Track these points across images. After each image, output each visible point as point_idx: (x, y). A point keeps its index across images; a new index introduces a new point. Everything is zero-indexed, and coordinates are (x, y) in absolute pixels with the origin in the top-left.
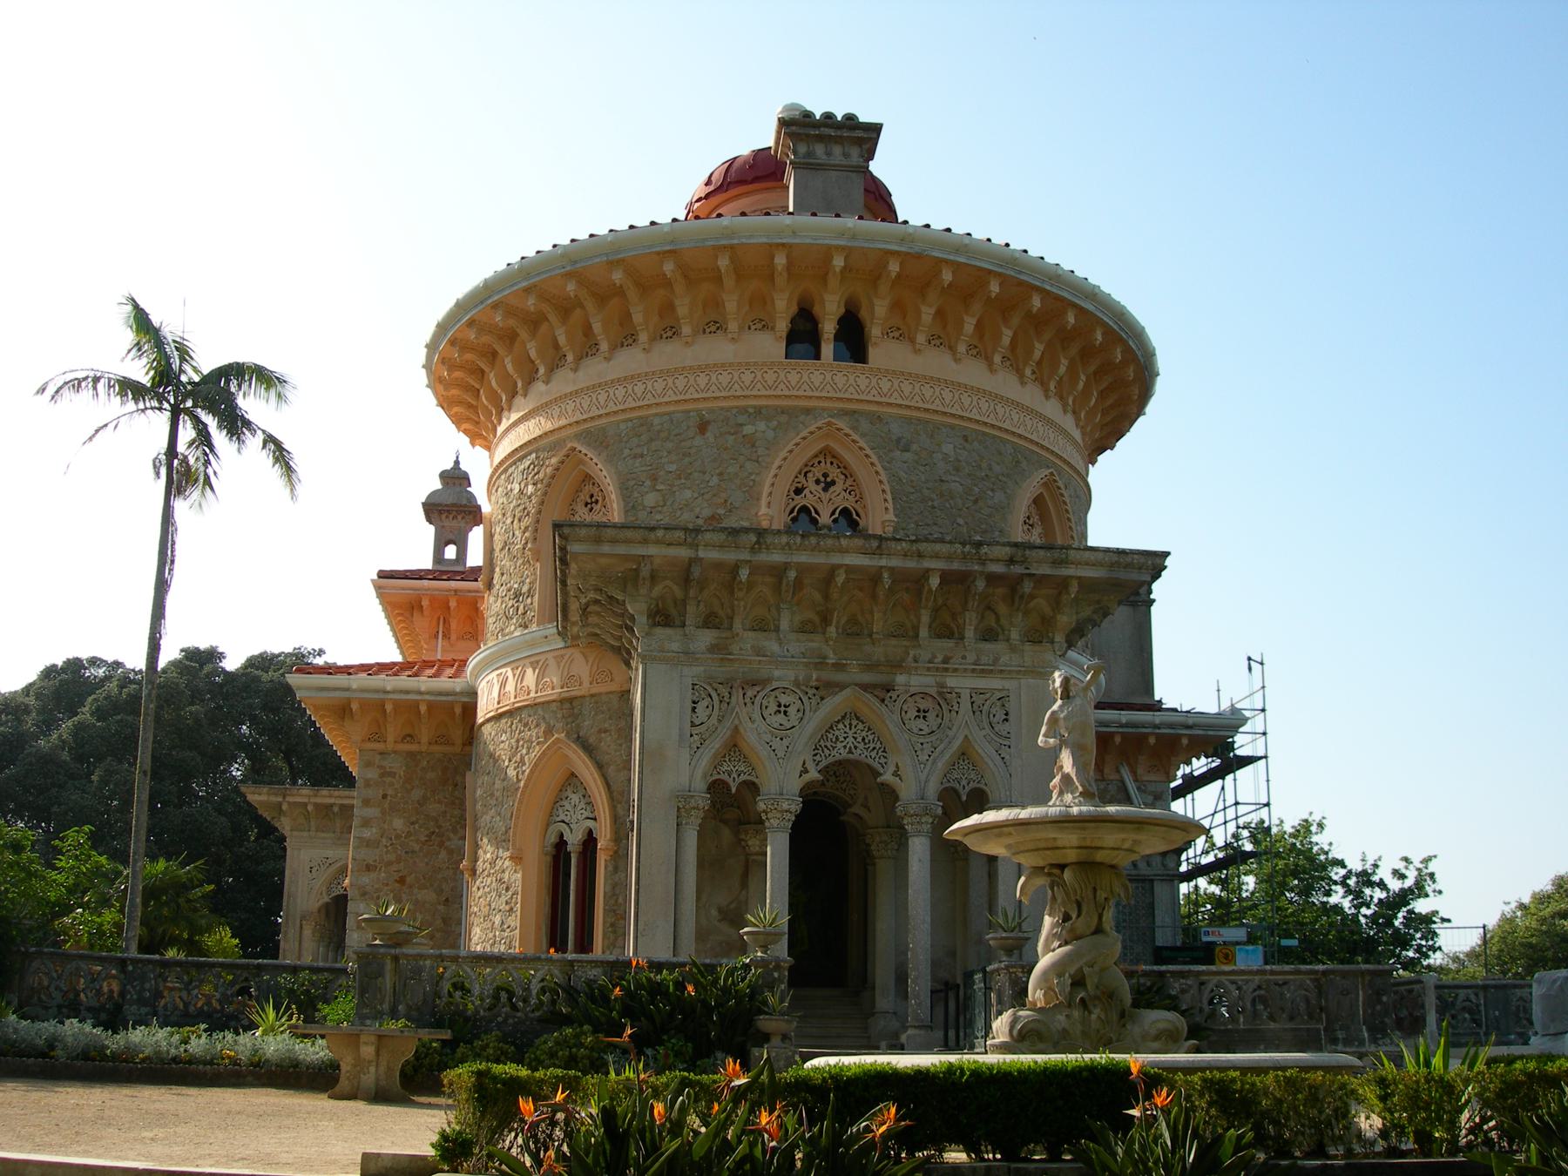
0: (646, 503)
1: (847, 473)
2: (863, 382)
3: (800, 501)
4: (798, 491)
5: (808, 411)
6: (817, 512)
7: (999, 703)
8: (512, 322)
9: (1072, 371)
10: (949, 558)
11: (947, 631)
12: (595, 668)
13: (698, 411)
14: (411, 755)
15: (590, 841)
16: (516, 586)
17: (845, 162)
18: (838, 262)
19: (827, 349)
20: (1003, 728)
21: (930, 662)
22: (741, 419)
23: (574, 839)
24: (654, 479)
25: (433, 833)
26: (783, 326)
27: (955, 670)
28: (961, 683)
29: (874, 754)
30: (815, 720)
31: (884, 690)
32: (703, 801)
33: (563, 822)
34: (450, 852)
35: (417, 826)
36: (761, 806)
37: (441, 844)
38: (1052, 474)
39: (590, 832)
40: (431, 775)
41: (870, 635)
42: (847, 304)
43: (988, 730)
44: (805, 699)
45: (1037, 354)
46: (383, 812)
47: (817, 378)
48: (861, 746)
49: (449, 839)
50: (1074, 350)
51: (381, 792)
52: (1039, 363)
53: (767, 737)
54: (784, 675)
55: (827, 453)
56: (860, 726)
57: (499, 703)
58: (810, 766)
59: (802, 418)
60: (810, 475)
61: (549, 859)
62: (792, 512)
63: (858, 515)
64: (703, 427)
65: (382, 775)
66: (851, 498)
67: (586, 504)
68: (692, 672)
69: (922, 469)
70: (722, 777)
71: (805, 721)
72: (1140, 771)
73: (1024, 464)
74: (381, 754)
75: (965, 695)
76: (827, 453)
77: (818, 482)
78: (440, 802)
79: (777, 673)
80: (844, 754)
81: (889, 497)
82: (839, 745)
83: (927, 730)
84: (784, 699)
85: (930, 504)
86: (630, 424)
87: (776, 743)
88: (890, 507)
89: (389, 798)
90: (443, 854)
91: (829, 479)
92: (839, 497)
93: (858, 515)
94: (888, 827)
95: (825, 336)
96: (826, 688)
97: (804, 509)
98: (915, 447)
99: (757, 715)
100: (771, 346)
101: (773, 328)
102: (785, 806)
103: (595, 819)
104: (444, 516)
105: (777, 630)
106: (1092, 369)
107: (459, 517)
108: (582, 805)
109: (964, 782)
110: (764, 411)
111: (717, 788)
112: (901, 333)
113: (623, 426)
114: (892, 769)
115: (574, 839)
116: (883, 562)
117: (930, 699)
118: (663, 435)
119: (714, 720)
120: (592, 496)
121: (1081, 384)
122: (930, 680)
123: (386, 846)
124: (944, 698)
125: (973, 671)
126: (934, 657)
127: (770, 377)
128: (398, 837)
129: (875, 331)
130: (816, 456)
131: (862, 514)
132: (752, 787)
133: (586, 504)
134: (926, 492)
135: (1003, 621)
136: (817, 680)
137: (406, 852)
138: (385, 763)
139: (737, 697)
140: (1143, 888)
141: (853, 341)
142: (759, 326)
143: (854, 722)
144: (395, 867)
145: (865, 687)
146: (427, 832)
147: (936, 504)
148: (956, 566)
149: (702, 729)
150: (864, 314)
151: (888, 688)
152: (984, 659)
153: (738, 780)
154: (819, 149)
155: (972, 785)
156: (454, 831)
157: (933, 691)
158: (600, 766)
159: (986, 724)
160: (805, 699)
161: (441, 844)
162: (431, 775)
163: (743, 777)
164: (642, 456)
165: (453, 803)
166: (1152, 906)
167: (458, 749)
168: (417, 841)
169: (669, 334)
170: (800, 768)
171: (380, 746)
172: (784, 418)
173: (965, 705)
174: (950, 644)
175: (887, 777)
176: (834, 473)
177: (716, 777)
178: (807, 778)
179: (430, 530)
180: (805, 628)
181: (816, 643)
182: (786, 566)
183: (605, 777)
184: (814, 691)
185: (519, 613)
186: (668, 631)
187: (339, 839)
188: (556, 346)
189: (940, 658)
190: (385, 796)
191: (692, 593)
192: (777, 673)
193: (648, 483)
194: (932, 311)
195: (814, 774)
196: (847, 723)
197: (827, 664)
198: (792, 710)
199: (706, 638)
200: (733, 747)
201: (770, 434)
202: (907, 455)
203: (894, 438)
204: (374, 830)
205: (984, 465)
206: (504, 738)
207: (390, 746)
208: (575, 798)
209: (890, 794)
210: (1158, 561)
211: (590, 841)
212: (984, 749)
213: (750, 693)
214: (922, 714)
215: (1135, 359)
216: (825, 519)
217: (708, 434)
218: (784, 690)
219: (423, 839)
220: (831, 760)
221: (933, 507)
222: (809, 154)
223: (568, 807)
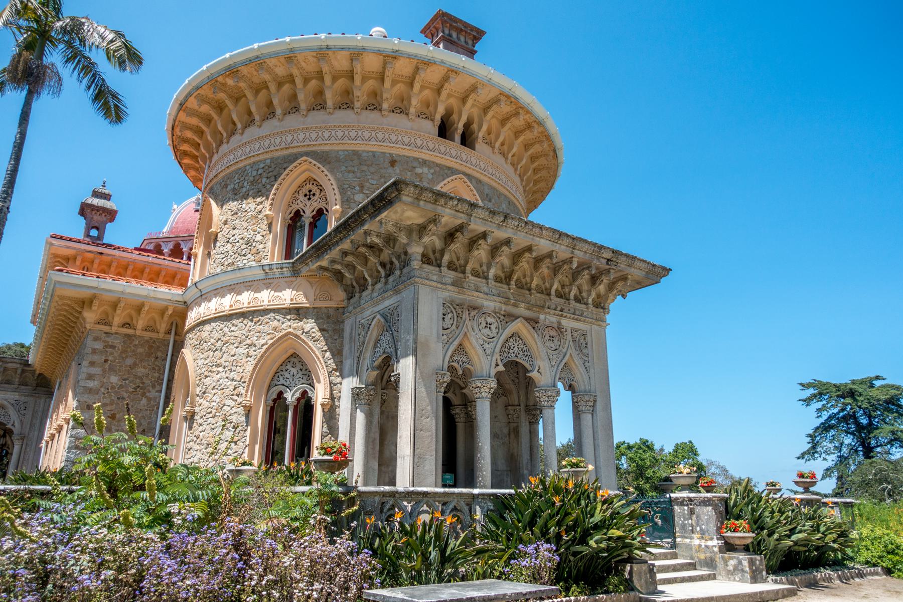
0: (355, 199)
5: (449, 168)
8: (267, 77)
12: (318, 292)
13: (391, 155)
14: (128, 336)
20: (585, 351)
22: (416, 164)
23: (291, 397)
24: (362, 187)
25: (139, 387)
26: (438, 118)
27: (565, 317)
29: (527, 358)
31: (533, 322)
33: (283, 385)
34: (149, 399)
35: (127, 382)
37: (143, 395)
40: (140, 350)
41: (530, 290)
46: (104, 371)
48: (521, 353)
49: (150, 392)
51: (104, 358)
56: (520, 341)
57: (231, 306)
59: (446, 171)
61: (269, 408)
64: (393, 163)
65: (106, 346)
67: (306, 195)
71: (499, 335)
74: (105, 333)
78: (145, 368)
79: (486, 303)
82: (511, 351)
83: (554, 348)
84: (489, 320)
87: (486, 345)
89: (109, 362)
90: (144, 401)
95: (459, 131)
96: (510, 317)
98: (493, 201)
100: (431, 128)
104: (94, 212)
105: (486, 278)
107: (103, 215)
108: (300, 375)
110: (427, 163)
111: (451, 369)
114: (537, 368)
115: (291, 397)
119: (454, 327)
120: (310, 191)
123: (104, 394)
124: (560, 329)
125: (573, 319)
126: (557, 307)
128: (113, 388)
129: (481, 135)
133: (306, 195)
135: (584, 294)
136: (505, 311)
137: (118, 398)
138: (107, 339)
139: (465, 315)
143: (518, 339)
144: (108, 408)
145: (527, 319)
146: (134, 386)
149: (448, 331)
152: (577, 313)
156: (154, 386)
157: (555, 326)
161: (143, 395)
162: (140, 350)
165: (154, 369)
167: (161, 336)
168: (127, 392)
169: (372, 108)
170: (494, 363)
171: (106, 328)
172: (438, 169)
173: (569, 337)
174: (563, 301)
179: (82, 222)
180: (497, 279)
184: (502, 317)
185: (252, 252)
186: (431, 268)
187: (35, 390)
188: (250, 113)
189: (559, 308)
190: (106, 361)
193: (357, 188)
195: (501, 368)
198: (493, 327)
199: (450, 275)
201: (430, 176)
204: (96, 382)
207: (114, 329)
208: (294, 371)
213: (473, 313)
218: (489, 315)
219: (131, 390)
220: (508, 359)
222: (450, 35)
223: (287, 375)
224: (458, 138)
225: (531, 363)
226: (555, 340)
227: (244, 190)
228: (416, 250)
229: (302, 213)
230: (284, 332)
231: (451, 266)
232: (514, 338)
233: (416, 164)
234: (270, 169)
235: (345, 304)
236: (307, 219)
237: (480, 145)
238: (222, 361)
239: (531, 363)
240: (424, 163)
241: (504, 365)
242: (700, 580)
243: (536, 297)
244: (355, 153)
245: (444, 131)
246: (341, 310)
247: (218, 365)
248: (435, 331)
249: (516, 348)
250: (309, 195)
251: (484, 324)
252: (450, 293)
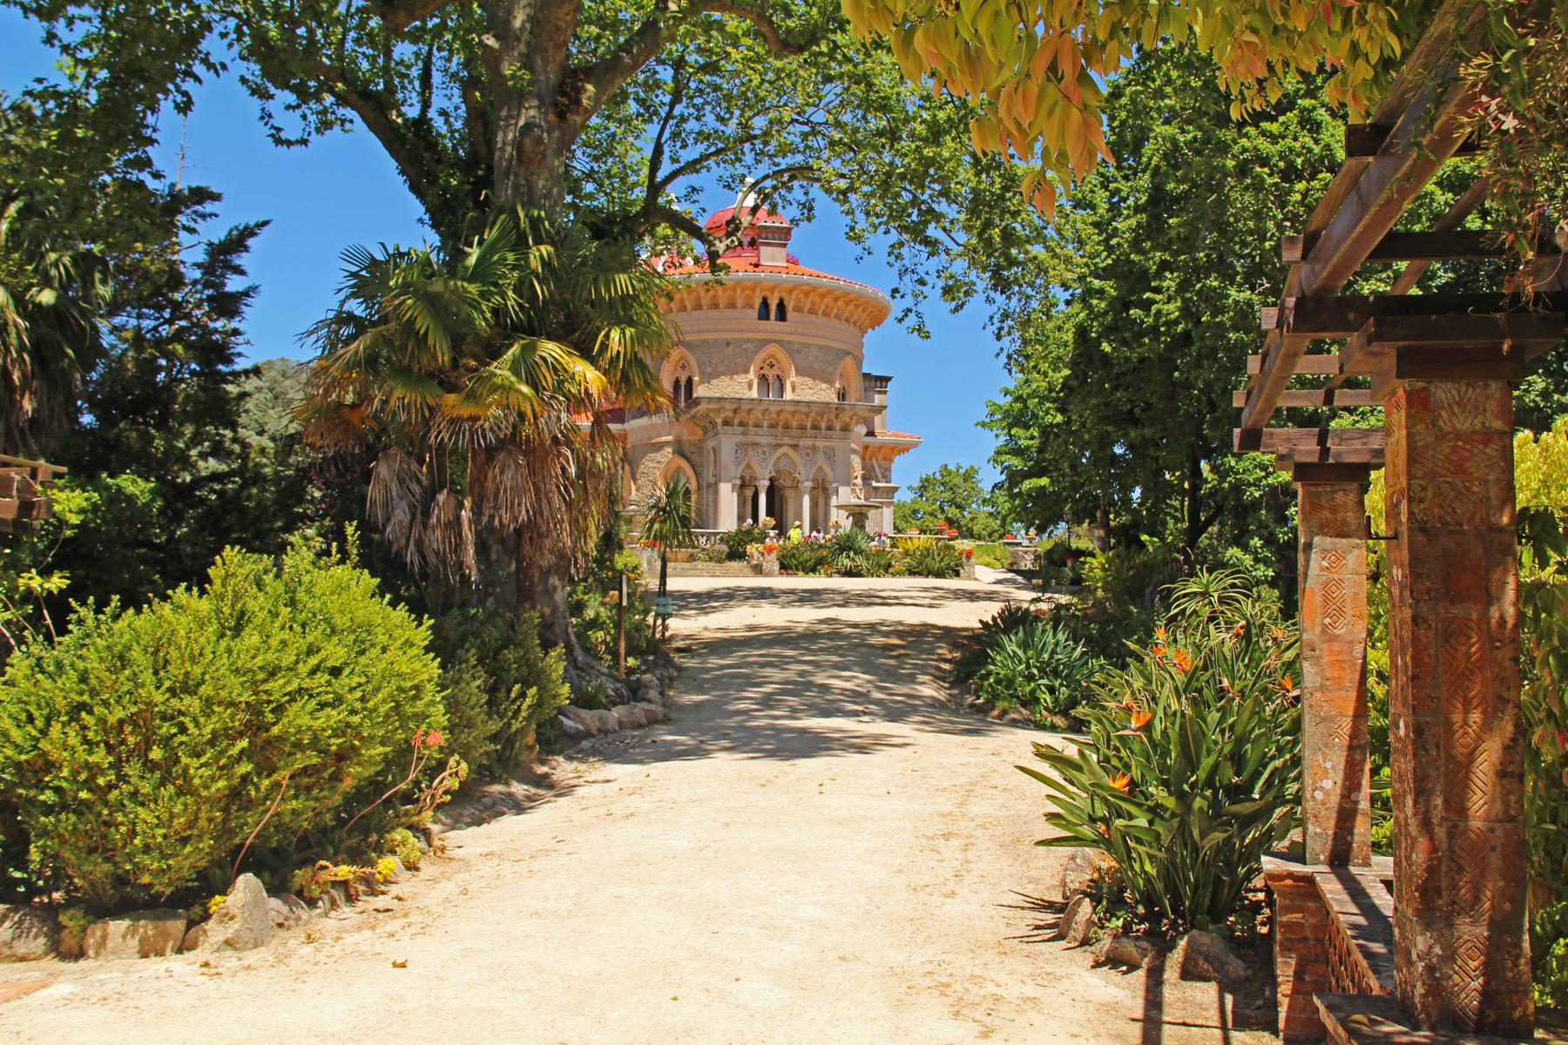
11: (815, 427)
28: (820, 444)
31: (795, 447)
32: (738, 482)
54: (765, 441)
92: (776, 371)
96: (780, 446)
111: (742, 478)
112: (798, 309)
124: (814, 448)
141: (782, 315)
158: (693, 466)
181: (774, 431)
200: (748, 466)
216: (771, 380)
224: (773, 316)
228: (719, 421)
231: (741, 424)
236: (683, 383)
237: (790, 315)
240: (748, 340)
242: (983, 599)
243: (794, 432)
244: (706, 341)
245: (764, 313)
250: (683, 367)
252: (740, 439)
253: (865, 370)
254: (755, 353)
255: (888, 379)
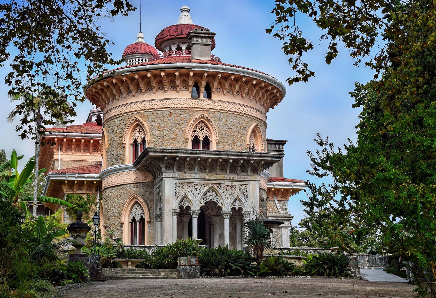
1: (207, 126)
2: (211, 103)
3: (195, 134)
4: (194, 131)
6: (199, 137)
7: (245, 188)
9: (263, 95)
10: (235, 155)
12: (143, 176)
15: (142, 219)
16: (118, 152)
17: (206, 43)
18: (206, 74)
19: (202, 96)
21: (229, 178)
22: (180, 113)
23: (138, 219)
29: (216, 199)
30: (203, 192)
36: (191, 212)
38: (257, 124)
39: (142, 217)
42: (207, 83)
43: (242, 194)
44: (201, 187)
45: (254, 93)
47: (199, 102)
48: (214, 198)
50: (264, 91)
52: (255, 95)
53: (193, 195)
55: (202, 121)
56: (213, 193)
58: (202, 202)
60: (198, 127)
61: (130, 224)
62: (193, 136)
63: (209, 137)
66: (207, 133)
68: (175, 181)
69: (225, 126)
70: (182, 205)
72: (279, 198)
73: (250, 122)
75: (237, 186)
76: (202, 121)
77: (199, 129)
80: (210, 200)
81: (217, 134)
82: (208, 197)
84: (196, 187)
85: (227, 134)
86: (151, 112)
88: (218, 136)
91: (202, 128)
93: (209, 137)
94: (217, 215)
96: (205, 185)
97: (196, 136)
99: (190, 191)
101: (188, 89)
102: (197, 212)
103: (144, 213)
106: (268, 94)
109: (237, 206)
111: (181, 208)
113: (149, 113)
115: (138, 219)
116: (220, 157)
117: (229, 187)
118: (160, 116)
121: (265, 98)
122: (230, 183)
126: (230, 177)
127: (188, 102)
129: (214, 90)
130: (199, 122)
131: (210, 137)
132: (188, 208)
134: (226, 131)
139: (185, 187)
140: (280, 230)
142: (185, 88)
143: (212, 192)
147: (229, 134)
148: (236, 157)
150: (211, 85)
151: (220, 184)
153: (186, 206)
154: (200, 40)
155: (239, 207)
157: (230, 185)
159: (242, 193)
160: (201, 187)
163: (187, 205)
164: (154, 121)
166: (282, 235)
172: (191, 113)
175: (219, 204)
176: (204, 126)
177: (181, 205)
178: (201, 205)
182: (198, 157)
183: (146, 203)
189: (232, 177)
191: (176, 163)
192: (194, 181)
193: (156, 128)
194: (228, 84)
196: (210, 192)
197: (206, 179)
198: (198, 190)
201: (188, 117)
202: (221, 122)
203: (219, 118)
205: (240, 124)
206: (116, 192)
209: (220, 208)
210: (282, 156)
211: (142, 219)
212: (242, 198)
214: (228, 190)
215: (280, 91)
216: (201, 139)
217: (172, 117)
221: (228, 135)
222: (197, 41)
225: (218, 201)
226: (230, 191)
227: (115, 130)
229: (137, 140)
230: (133, 193)
232: (210, 192)
233: (180, 113)
234: (124, 121)
235: (153, 181)
238: (113, 205)
239: (218, 201)
241: (205, 204)
246: (152, 183)
247: (112, 207)
248: (172, 195)
249: (211, 196)
251: (194, 189)
253: (268, 137)
254: (189, 120)
255: (283, 143)
